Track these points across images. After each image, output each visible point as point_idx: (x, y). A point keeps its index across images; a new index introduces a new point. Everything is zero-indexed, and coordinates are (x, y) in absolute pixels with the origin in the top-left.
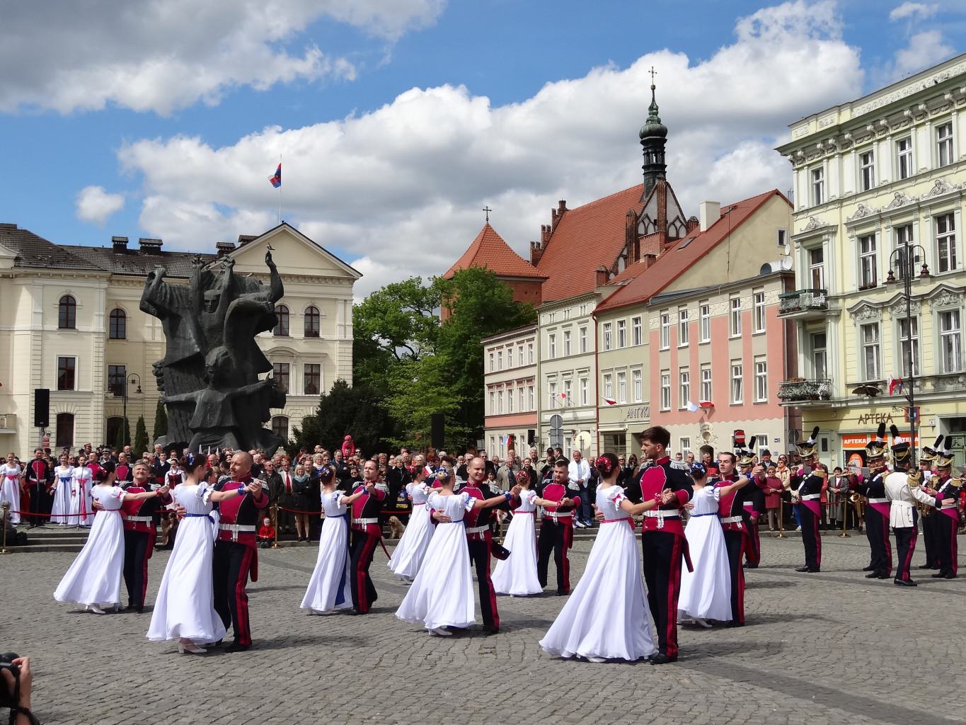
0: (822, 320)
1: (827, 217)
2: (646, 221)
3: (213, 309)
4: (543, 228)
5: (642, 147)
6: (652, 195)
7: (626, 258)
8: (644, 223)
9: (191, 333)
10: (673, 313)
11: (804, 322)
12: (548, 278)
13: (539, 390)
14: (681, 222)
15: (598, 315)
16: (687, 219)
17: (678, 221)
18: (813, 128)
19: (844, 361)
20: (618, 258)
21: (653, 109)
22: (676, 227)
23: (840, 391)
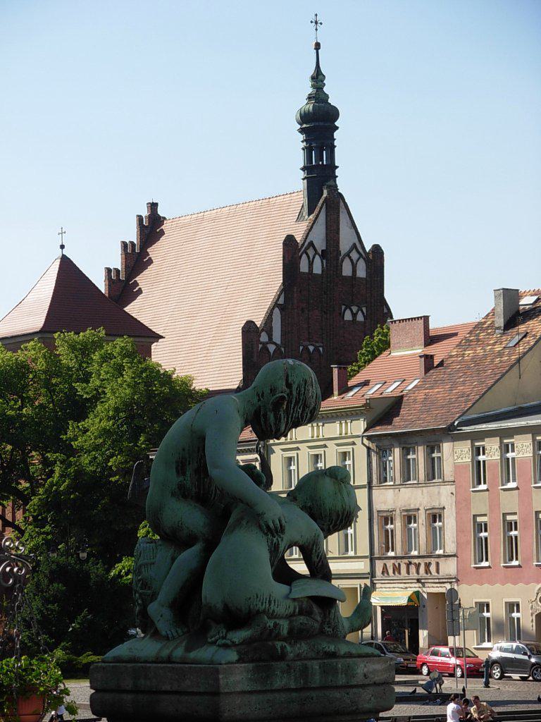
2: (311, 252)
4: (125, 245)
5: (302, 137)
6: (320, 212)
7: (282, 308)
8: (307, 254)
12: (162, 337)
14: (358, 252)
16: (368, 248)
17: (354, 251)
20: (273, 309)
21: (318, 78)
22: (351, 260)
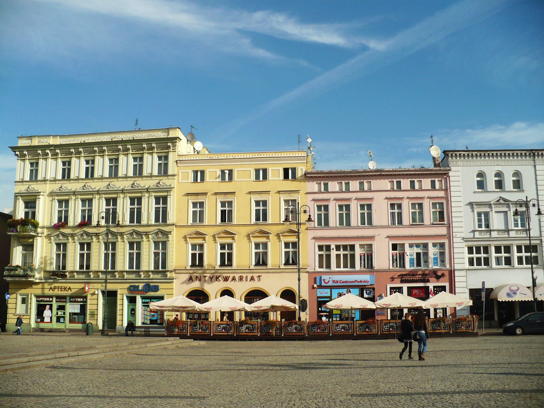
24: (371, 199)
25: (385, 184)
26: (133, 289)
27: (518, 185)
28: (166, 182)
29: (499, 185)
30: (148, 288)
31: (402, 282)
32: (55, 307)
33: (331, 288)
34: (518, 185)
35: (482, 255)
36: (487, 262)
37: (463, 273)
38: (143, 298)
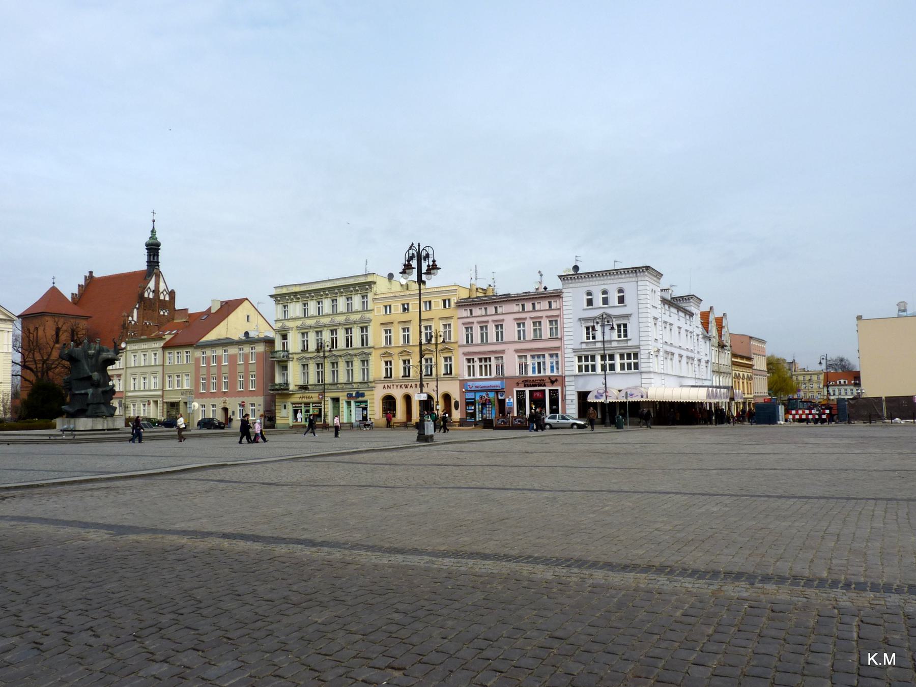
0: (286, 361)
1: (290, 324)
3: (91, 358)
4: (79, 286)
9: (86, 367)
10: (209, 353)
11: (279, 362)
13: (126, 381)
15: (164, 348)
18: (284, 291)
19: (294, 376)
21: (153, 231)
23: (292, 387)
24: (503, 320)
25: (515, 307)
26: (350, 396)
27: (621, 300)
28: (368, 315)
29: (605, 301)
30: (359, 395)
31: (525, 386)
32: (303, 411)
33: (475, 391)
34: (621, 300)
35: (590, 363)
36: (594, 368)
37: (573, 379)
38: (356, 402)
